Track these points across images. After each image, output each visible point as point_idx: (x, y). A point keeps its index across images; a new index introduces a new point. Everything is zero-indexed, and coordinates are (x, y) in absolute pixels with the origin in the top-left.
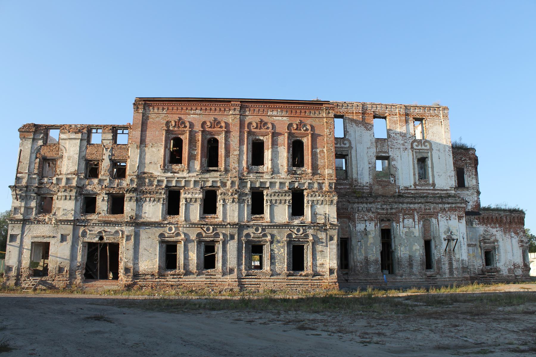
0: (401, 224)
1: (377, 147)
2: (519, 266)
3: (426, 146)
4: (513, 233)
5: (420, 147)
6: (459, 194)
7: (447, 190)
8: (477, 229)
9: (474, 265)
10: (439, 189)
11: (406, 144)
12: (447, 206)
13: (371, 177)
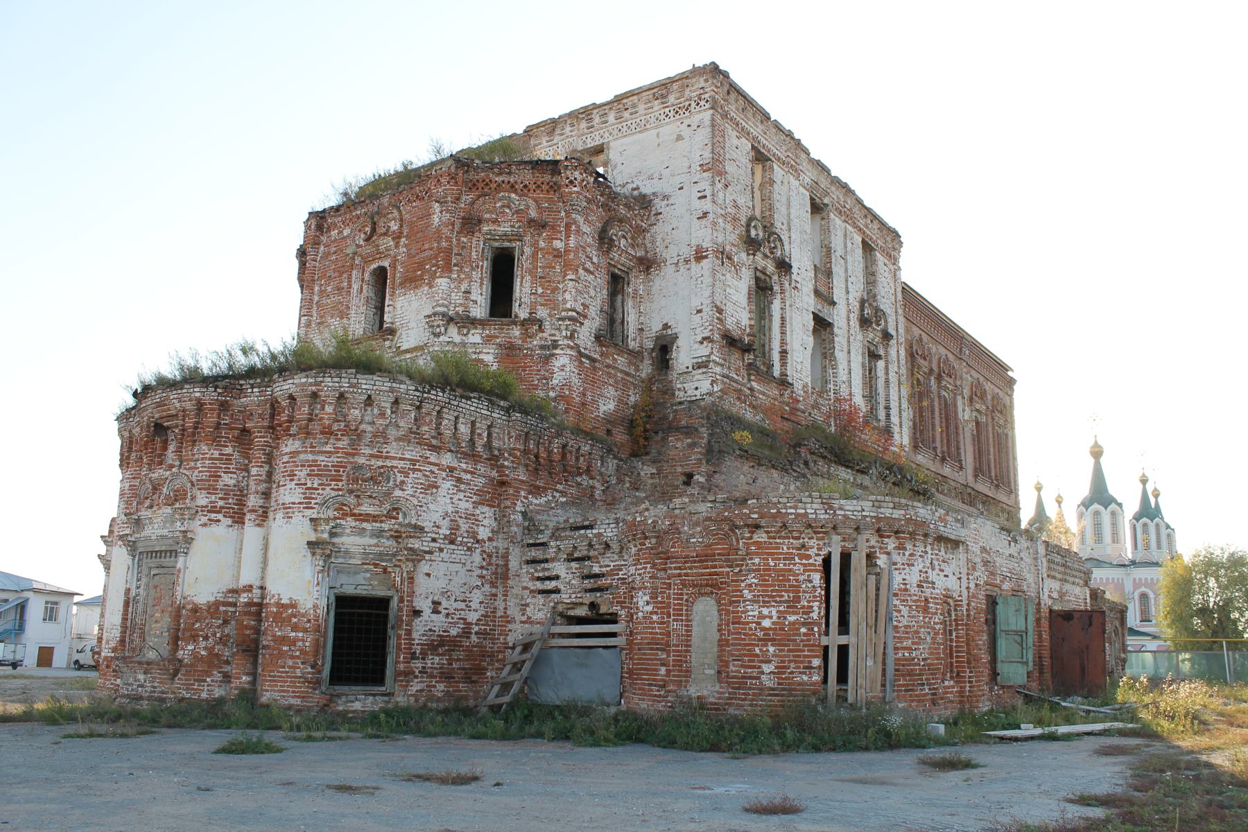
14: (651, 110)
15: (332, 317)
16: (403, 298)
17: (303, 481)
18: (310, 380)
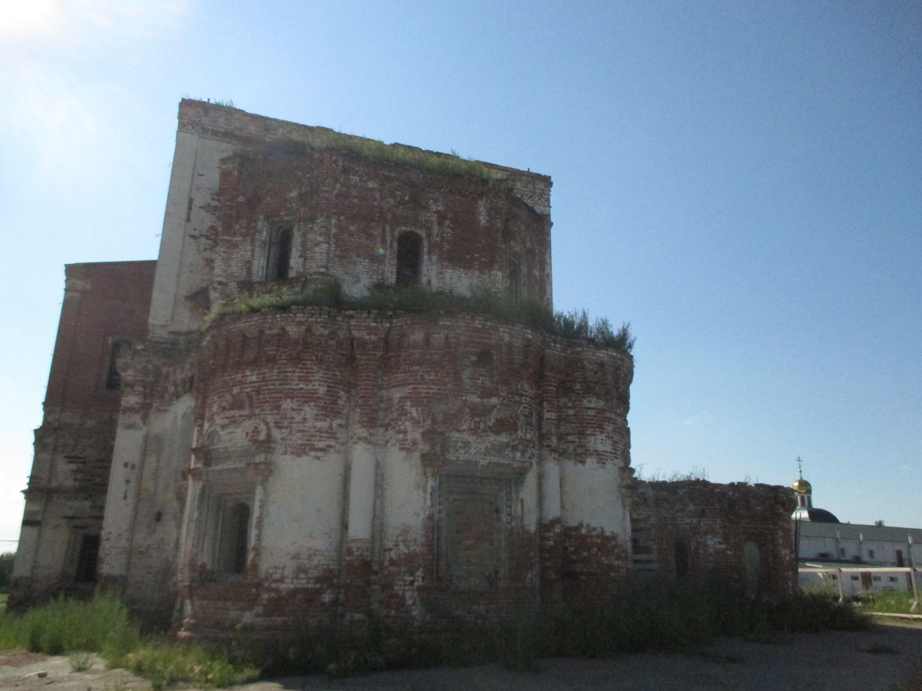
15: (359, 256)
16: (452, 271)
17: (611, 435)
18: (619, 356)
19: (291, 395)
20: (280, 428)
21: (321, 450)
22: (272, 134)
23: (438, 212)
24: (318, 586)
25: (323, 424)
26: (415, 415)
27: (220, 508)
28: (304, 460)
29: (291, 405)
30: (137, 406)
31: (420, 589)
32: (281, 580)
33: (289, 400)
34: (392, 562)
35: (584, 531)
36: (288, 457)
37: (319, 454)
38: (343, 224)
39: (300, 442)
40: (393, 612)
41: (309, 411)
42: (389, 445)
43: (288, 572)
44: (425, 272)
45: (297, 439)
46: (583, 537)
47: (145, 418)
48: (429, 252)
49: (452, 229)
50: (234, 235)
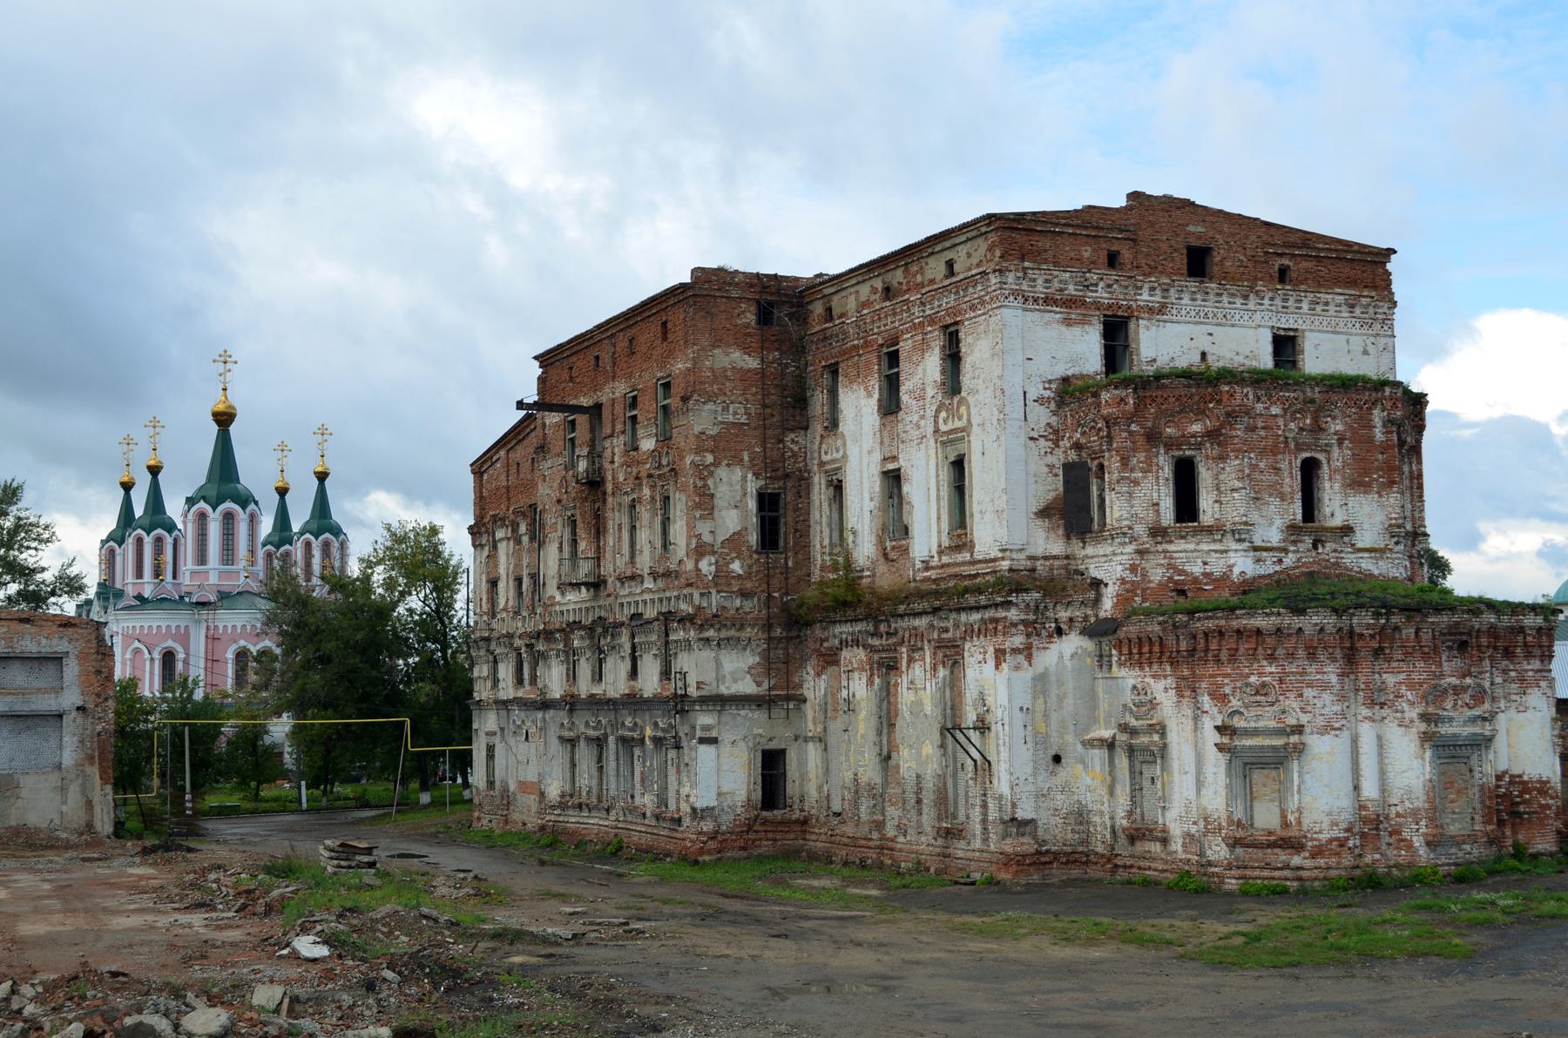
0: (904, 677)
1: (882, 443)
2: (1220, 824)
3: (960, 418)
4: (1206, 698)
5: (950, 426)
6: (1087, 557)
7: (994, 560)
8: (1120, 681)
9: (1102, 813)
10: (981, 557)
11: (922, 423)
12: (975, 617)
13: (874, 539)
14: (1339, 315)
15: (1270, 496)
19: (1310, 685)
20: (1306, 712)
21: (1339, 729)
22: (1092, 291)
23: (1336, 433)
24: (1346, 835)
25: (1337, 708)
26: (1410, 697)
27: (1245, 776)
28: (1327, 738)
29: (1312, 694)
30: (1021, 646)
31: (1424, 835)
32: (1321, 832)
33: (1310, 689)
34: (1398, 815)
35: (1525, 778)
36: (1316, 736)
37: (1338, 732)
38: (1254, 462)
39: (1323, 724)
40: (1403, 852)
41: (1327, 697)
42: (1386, 721)
43: (1325, 826)
44: (1326, 502)
45: (1320, 721)
46: (1524, 783)
47: (1029, 658)
48: (1330, 479)
49: (1351, 449)
50: (1132, 470)
